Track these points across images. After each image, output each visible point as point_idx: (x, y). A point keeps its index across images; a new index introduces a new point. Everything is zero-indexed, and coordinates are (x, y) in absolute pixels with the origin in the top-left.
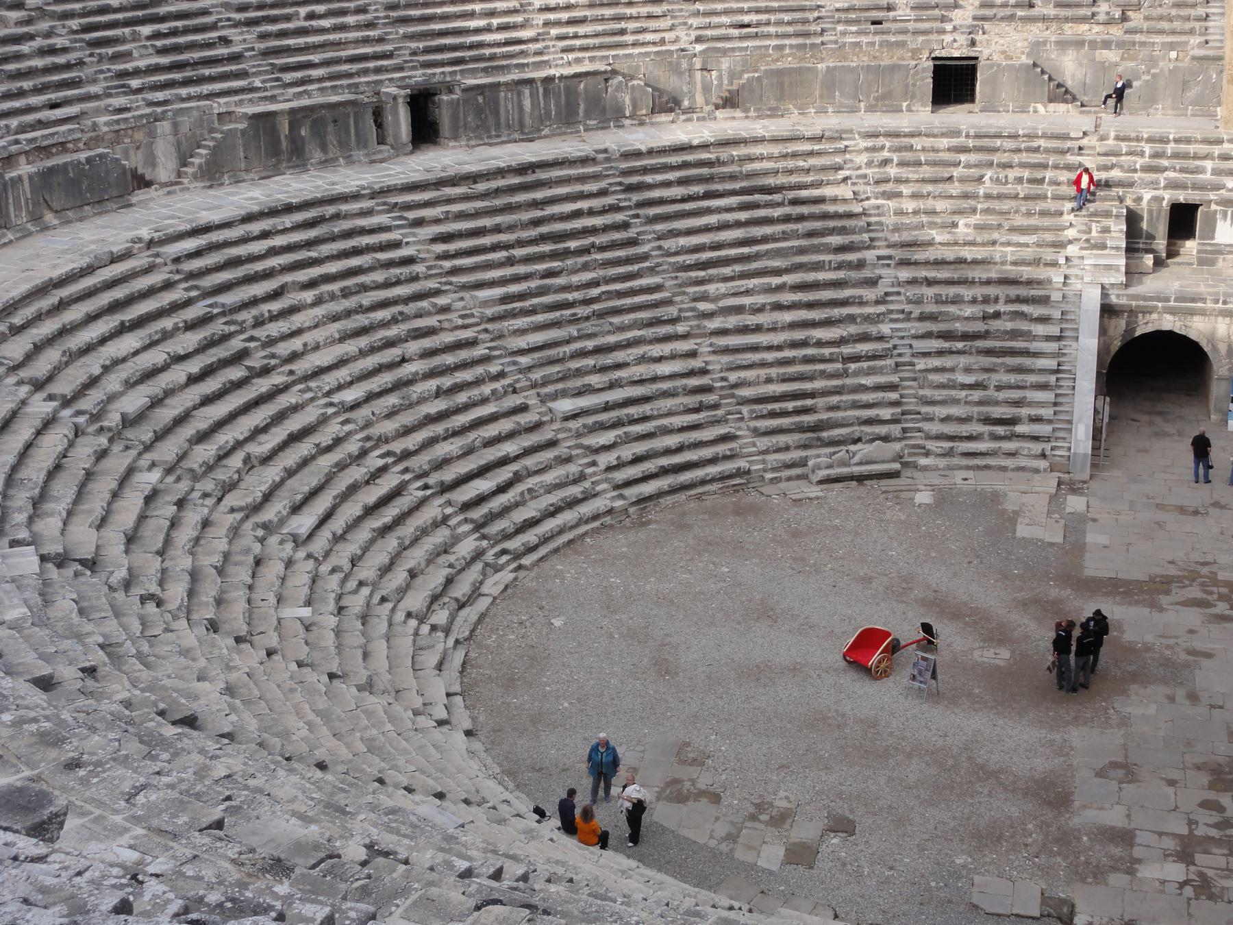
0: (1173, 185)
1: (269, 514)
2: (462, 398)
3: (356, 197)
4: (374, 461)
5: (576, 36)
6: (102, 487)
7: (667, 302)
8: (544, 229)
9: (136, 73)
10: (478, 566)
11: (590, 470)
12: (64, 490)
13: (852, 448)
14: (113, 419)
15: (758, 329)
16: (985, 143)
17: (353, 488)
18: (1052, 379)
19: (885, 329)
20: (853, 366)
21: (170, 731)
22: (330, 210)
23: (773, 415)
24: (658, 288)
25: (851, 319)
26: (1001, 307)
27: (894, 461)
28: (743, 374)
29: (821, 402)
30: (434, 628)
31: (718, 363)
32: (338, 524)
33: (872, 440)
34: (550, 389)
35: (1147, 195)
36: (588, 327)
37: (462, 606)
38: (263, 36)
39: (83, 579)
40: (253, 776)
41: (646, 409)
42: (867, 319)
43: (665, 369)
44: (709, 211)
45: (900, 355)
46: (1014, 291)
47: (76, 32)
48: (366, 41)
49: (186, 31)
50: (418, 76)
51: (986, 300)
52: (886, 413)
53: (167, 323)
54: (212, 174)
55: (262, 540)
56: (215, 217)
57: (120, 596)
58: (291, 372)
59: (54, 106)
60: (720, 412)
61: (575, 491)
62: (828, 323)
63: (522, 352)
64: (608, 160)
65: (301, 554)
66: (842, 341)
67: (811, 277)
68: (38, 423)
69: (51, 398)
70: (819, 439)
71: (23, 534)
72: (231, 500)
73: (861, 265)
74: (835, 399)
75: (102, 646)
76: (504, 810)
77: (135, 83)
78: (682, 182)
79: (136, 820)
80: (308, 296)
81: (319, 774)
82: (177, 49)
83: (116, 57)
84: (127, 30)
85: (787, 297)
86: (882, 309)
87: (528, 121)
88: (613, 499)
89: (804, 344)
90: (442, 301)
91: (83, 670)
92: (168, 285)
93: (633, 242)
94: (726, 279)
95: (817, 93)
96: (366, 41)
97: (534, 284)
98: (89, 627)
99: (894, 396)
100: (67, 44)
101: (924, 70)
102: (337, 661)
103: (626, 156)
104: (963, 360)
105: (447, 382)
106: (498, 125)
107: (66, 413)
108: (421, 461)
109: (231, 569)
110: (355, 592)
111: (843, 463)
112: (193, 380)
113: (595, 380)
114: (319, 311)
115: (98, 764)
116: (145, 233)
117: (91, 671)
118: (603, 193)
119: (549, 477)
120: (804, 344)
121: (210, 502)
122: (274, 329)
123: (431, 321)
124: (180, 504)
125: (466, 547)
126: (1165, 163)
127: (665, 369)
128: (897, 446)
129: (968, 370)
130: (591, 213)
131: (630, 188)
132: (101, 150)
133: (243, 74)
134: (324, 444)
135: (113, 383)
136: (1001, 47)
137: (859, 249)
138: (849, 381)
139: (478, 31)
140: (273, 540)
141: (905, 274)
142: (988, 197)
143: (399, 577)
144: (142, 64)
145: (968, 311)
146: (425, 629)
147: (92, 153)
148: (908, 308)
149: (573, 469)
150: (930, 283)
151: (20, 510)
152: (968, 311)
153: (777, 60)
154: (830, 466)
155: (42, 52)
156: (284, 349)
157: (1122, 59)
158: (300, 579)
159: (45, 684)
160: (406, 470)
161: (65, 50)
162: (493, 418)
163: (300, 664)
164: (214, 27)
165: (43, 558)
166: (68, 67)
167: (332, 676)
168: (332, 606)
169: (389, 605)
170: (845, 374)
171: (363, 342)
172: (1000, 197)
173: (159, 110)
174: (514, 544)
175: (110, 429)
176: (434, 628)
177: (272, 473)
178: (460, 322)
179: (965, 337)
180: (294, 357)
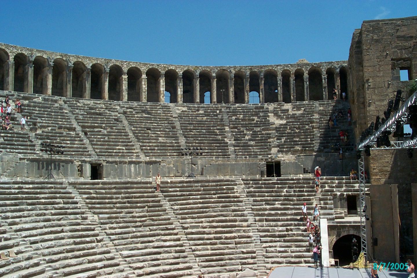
7: (172, 224)
13: (238, 273)
15: (204, 233)
19: (251, 234)
23: (207, 261)
29: (227, 257)
35: (339, 194)
41: (158, 256)
42: (244, 231)
45: (256, 242)
52: (251, 261)
66: (234, 238)
70: (226, 269)
85: (214, 224)
87: (133, 175)
95: (229, 172)
99: (254, 255)
101: (263, 164)
104: (278, 244)
129: (281, 247)
136: (286, 158)
137: (242, 211)
145: (280, 228)
152: (280, 228)
153: (216, 162)
157: (325, 160)
179: (280, 236)
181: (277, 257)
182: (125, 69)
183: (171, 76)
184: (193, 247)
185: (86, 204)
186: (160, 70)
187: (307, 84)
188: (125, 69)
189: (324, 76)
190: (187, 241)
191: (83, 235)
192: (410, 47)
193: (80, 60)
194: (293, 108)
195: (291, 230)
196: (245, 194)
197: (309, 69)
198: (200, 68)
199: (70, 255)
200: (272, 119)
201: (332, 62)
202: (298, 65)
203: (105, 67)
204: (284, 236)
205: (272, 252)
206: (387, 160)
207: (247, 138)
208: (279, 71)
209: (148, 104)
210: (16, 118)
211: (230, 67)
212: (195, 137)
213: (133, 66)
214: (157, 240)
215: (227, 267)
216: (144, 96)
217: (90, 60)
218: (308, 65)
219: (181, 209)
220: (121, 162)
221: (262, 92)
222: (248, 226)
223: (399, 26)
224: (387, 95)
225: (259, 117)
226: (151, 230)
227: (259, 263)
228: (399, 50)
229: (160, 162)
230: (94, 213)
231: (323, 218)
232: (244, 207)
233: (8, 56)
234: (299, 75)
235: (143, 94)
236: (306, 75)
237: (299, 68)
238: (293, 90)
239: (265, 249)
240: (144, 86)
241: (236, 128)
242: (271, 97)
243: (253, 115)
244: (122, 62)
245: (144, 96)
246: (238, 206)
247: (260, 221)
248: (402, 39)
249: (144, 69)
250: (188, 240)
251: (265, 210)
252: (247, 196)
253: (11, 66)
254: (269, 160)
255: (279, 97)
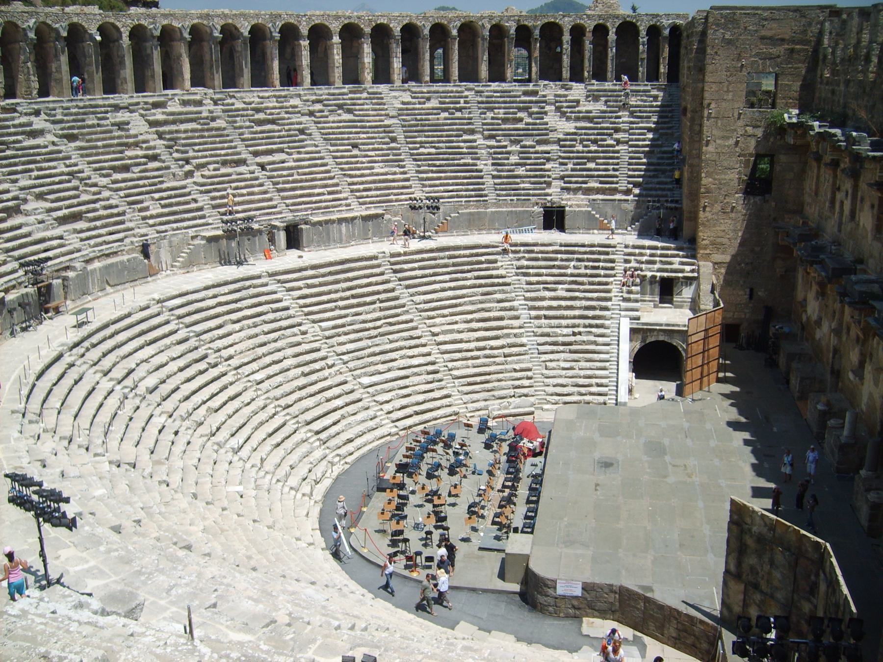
0: (659, 270)
1: (221, 436)
2: (314, 377)
3: (259, 277)
4: (270, 410)
5: (367, 197)
6: (137, 425)
7: (416, 328)
8: (353, 292)
9: (152, 217)
10: (324, 462)
11: (379, 413)
12: (118, 428)
13: (510, 400)
14: (141, 389)
15: (461, 341)
16: (569, 249)
17: (262, 424)
18: (607, 364)
19: (524, 340)
20: (509, 359)
21: (182, 553)
22: (248, 283)
23: (469, 384)
24: (411, 321)
25: (508, 336)
26: (581, 329)
27: (531, 406)
28: (455, 363)
30: (304, 495)
31: (440, 358)
32: (253, 442)
33: (520, 397)
34: (358, 372)
35: (649, 274)
36: (377, 340)
37: (317, 483)
38: (213, 199)
39: (129, 473)
40: (225, 577)
41: (406, 382)
42: (515, 335)
43: (415, 361)
44: (435, 282)
46: (587, 322)
47: (122, 198)
48: (263, 200)
49: (176, 196)
50: (289, 216)
51: (574, 326)
52: (526, 382)
53: (167, 341)
54: (189, 265)
55: (217, 452)
56: (190, 288)
57: (149, 481)
58: (229, 365)
59: (111, 234)
60: (443, 383)
61: (371, 424)
62: (497, 338)
63: (344, 354)
64: (384, 257)
65: (236, 458)
66: (503, 347)
67: (486, 315)
68: (105, 393)
69: (111, 380)
71: (100, 450)
72: (202, 430)
73: (511, 309)
74: (500, 376)
75: (142, 509)
76: (345, 589)
77: (151, 222)
78: (420, 268)
79: (172, 603)
80: (237, 326)
81: (254, 574)
82: (171, 205)
83: (140, 210)
84: (147, 196)
85: (475, 325)
86: (522, 330)
87: (344, 238)
88: (391, 428)
89: (484, 348)
90: (303, 328)
91: (134, 521)
92: (167, 322)
93: (397, 298)
94: (444, 316)
96: (263, 200)
97: (349, 319)
98: (136, 499)
99: (529, 374)
100: (118, 203)
101: (539, 213)
102: (257, 513)
103: (393, 255)
104: (562, 356)
105: (306, 369)
106: (329, 239)
107: (118, 387)
108: (293, 410)
109: (201, 466)
110: (264, 477)
111: (506, 408)
112: (181, 370)
113: (381, 367)
114: (242, 334)
115: (150, 574)
116: (157, 296)
117: (138, 522)
118: (382, 274)
119: (359, 417)
120: (484, 348)
121: (190, 432)
122: (219, 344)
123: (299, 338)
124: (176, 433)
125: (318, 454)
126: (658, 259)
127: (415, 361)
128: (532, 399)
130: (377, 284)
131: (395, 271)
132: (134, 255)
133: (203, 217)
134: (246, 402)
135: (141, 372)
136: (575, 203)
137: (510, 301)
138: (507, 367)
139: (319, 195)
140: (222, 451)
141: (534, 313)
142: (572, 275)
143: (285, 467)
144: (154, 212)
145: (566, 331)
146: (299, 495)
147: (130, 257)
148: (536, 330)
149: (371, 413)
150: (546, 317)
151: (98, 437)
154: (499, 409)
155: (106, 208)
156: (225, 353)
158: (236, 472)
159: (117, 529)
160: (288, 414)
161: (117, 206)
162: (330, 388)
163: (239, 515)
164: (189, 194)
165: (110, 462)
166: (118, 215)
167: (254, 521)
168: (253, 485)
169: (281, 484)
170: (506, 363)
171: (264, 350)
172: (579, 275)
173: (163, 234)
174: (343, 451)
175: (140, 396)
176: (304, 495)
177: (221, 416)
178: (312, 339)
179: (564, 344)
180: (231, 357)
181: (561, 376)
182: (304, 30)
183: (381, 33)
184: (450, 365)
185: (293, 299)
186: (362, 26)
187: (612, 52)
188: (304, 30)
189: (643, 38)
190: (440, 355)
191: (309, 361)
192: (779, 57)
193: (230, 21)
194: (588, 97)
195: (580, 333)
196: (513, 271)
197: (618, 24)
198: (431, 19)
199: (303, 393)
200: (552, 119)
201: (657, 15)
202: (600, 16)
203: (272, 30)
204: (570, 344)
205: (554, 369)
206: (723, 228)
207: (514, 159)
208: (567, 23)
209: (345, 90)
210: (159, 155)
211: (482, 18)
212: (429, 157)
213: (316, 22)
214: (402, 357)
215: (496, 393)
216: (337, 73)
217: (245, 19)
218: (617, 18)
219: (426, 302)
220: (327, 222)
221: (536, 63)
222: (520, 327)
223: (766, 20)
224: (735, 130)
225: (530, 115)
226: (391, 342)
227: (537, 386)
228: (761, 59)
229: (383, 214)
230: (314, 322)
231: (625, 316)
232: (513, 294)
233: (121, 33)
234: (601, 30)
235: (336, 70)
236: (612, 36)
237: (601, 22)
238: (589, 61)
239: (543, 364)
240: (336, 57)
241: (492, 137)
242: (550, 72)
243: (520, 109)
244: (298, 16)
245: (337, 75)
246: (504, 292)
247: (538, 318)
248: (768, 41)
249: (335, 27)
250: (442, 353)
251: (543, 299)
252: (517, 274)
253: (126, 51)
254: (549, 205)
255: (564, 72)
